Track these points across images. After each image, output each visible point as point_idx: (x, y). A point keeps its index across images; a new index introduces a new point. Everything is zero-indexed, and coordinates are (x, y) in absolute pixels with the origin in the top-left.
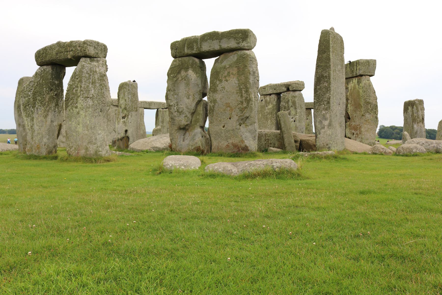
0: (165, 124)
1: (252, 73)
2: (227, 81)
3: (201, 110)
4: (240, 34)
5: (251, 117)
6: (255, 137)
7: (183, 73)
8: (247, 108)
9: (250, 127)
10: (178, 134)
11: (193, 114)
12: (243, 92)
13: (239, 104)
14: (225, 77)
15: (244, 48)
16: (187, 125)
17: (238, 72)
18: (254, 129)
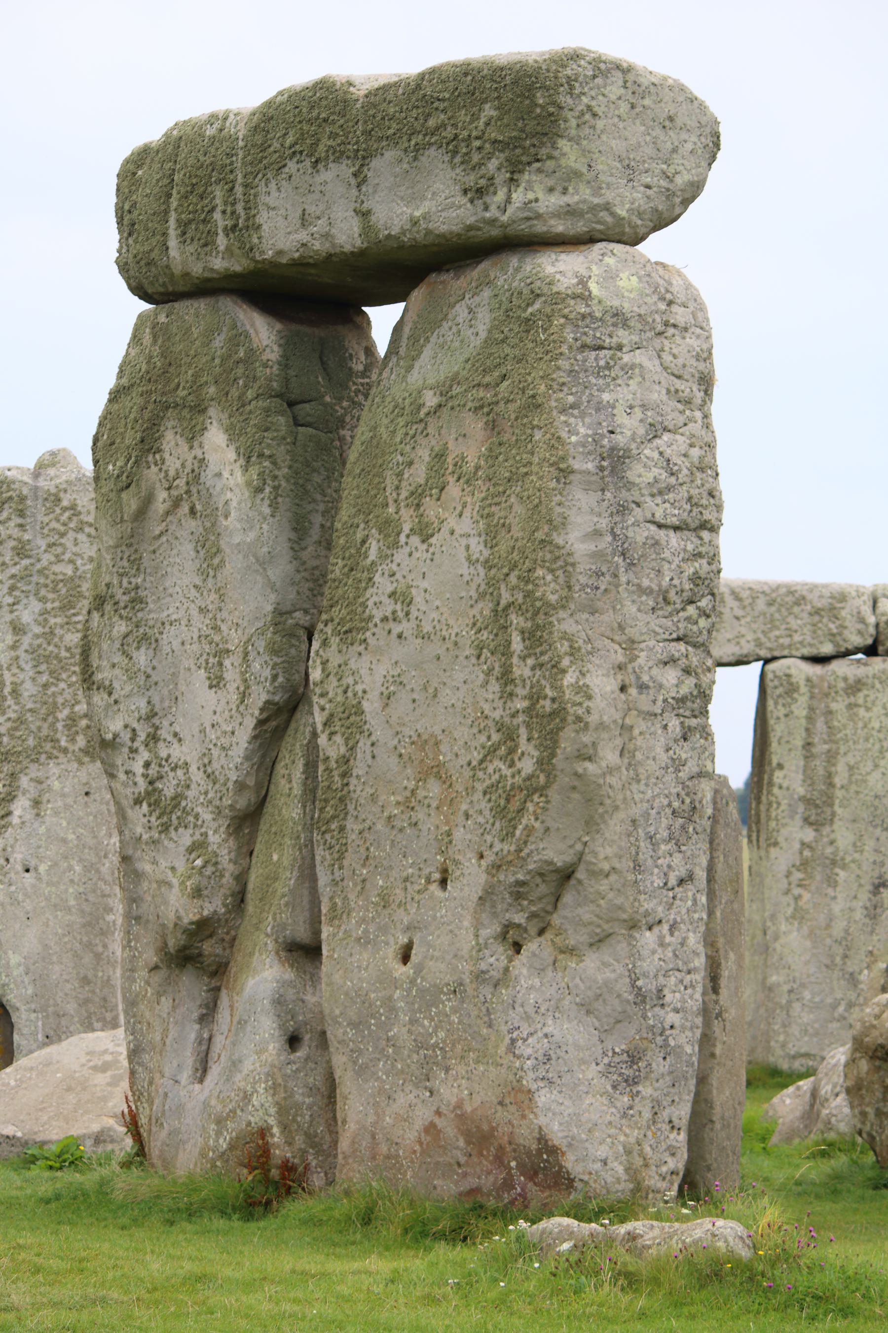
0: (843, 835)
1: (586, 465)
2: (424, 532)
3: (297, 790)
4: (489, 111)
5: (595, 874)
6: (633, 1057)
7: (174, 450)
8: (541, 790)
9: (593, 968)
10: (166, 1003)
11: (247, 821)
12: (517, 644)
13: (494, 749)
14: (417, 497)
15: (540, 228)
16: (203, 928)
17: (492, 456)
18: (623, 986)
